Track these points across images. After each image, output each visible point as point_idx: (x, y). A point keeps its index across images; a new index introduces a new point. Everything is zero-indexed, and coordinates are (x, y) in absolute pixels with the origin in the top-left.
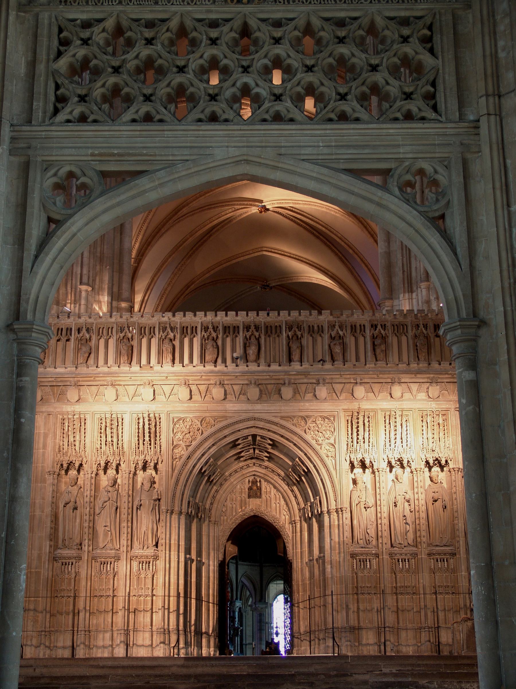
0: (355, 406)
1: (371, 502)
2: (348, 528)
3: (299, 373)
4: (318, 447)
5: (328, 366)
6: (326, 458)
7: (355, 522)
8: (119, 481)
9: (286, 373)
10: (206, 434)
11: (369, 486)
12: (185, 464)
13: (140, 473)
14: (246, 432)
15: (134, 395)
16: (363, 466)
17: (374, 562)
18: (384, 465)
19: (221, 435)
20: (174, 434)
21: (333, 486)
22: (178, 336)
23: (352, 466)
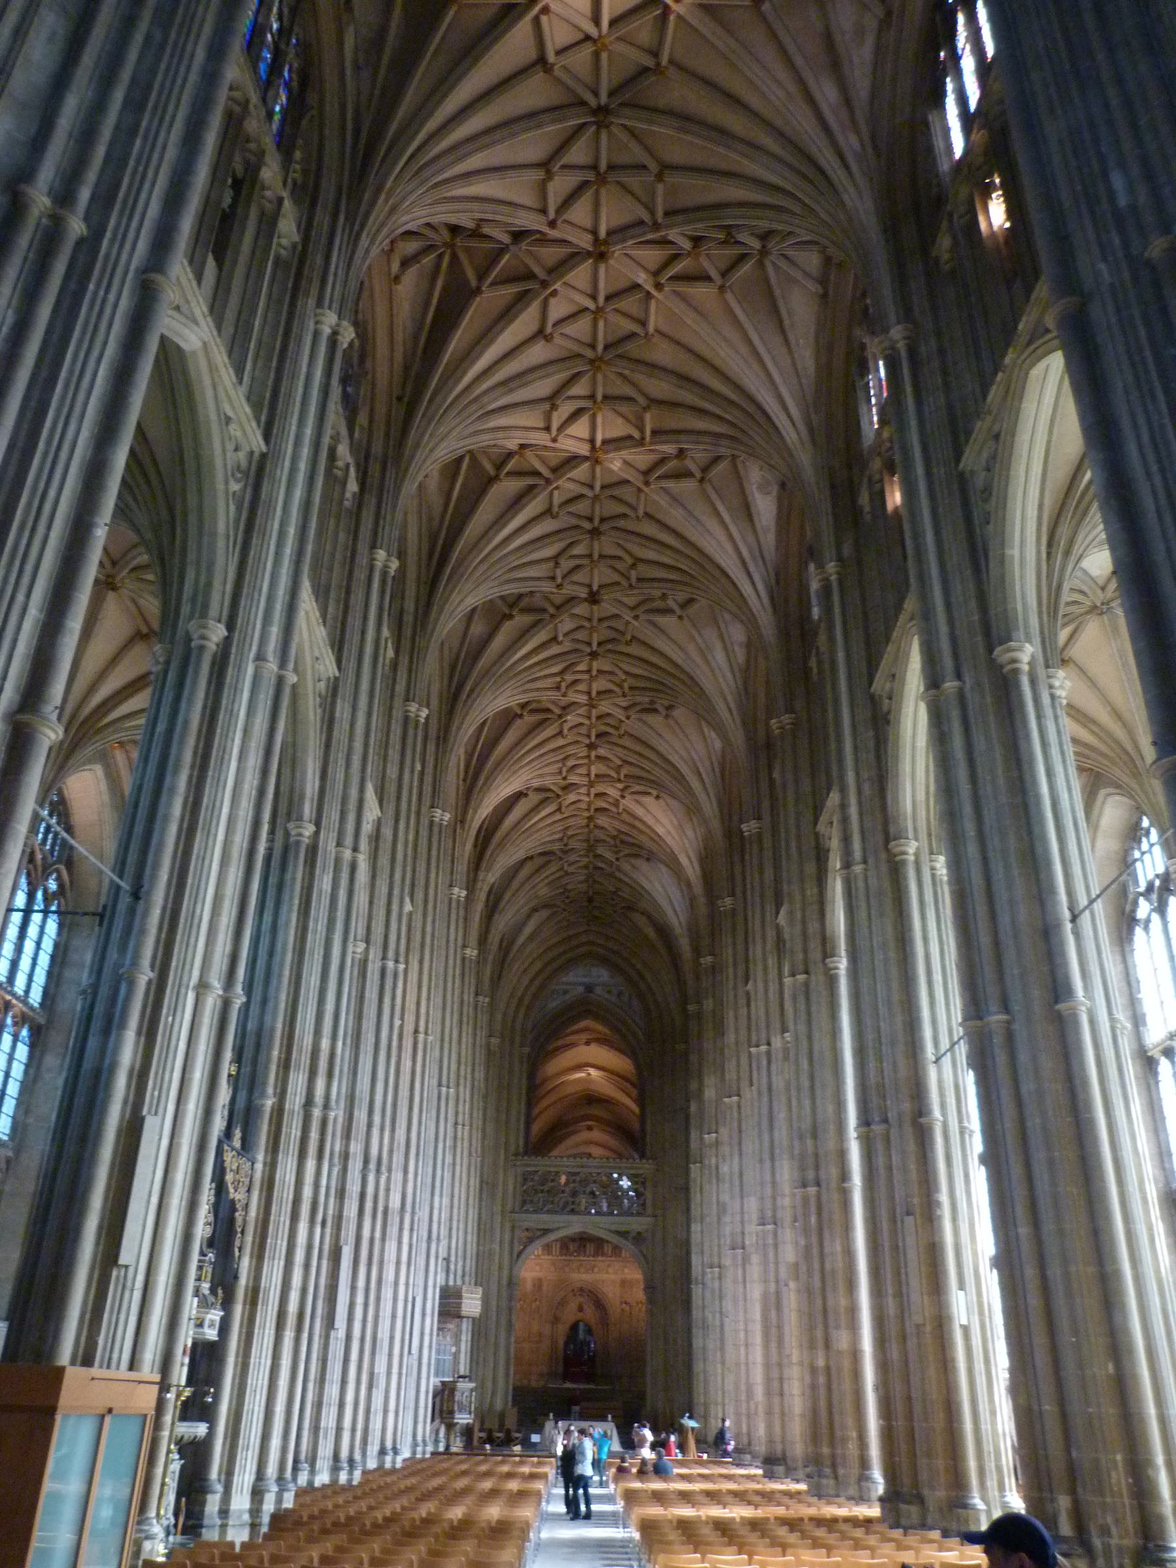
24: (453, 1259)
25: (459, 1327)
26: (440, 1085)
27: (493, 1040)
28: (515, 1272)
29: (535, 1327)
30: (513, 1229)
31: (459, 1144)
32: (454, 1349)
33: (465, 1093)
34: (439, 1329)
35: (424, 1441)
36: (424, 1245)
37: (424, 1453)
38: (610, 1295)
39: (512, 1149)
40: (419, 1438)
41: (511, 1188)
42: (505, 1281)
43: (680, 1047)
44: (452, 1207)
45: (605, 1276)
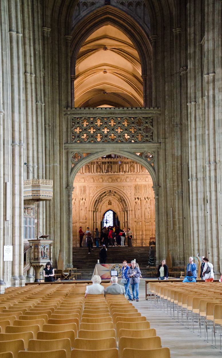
0: (136, 183)
1: (140, 208)
2: (134, 215)
3: (122, 175)
4: (127, 194)
5: (129, 173)
6: (129, 197)
7: (136, 213)
8: (76, 203)
9: (118, 175)
10: (98, 190)
11: (140, 204)
12: (93, 198)
13: (81, 200)
14: (108, 190)
15: (79, 180)
16: (138, 199)
17: (140, 223)
18: (143, 199)
19: (101, 191)
20: (90, 191)
21: (130, 204)
22: (90, 165)
23: (135, 199)
24: (31, 163)
25: (38, 206)
26: (10, 30)
27: (46, 29)
28: (70, 179)
29: (83, 213)
30: (67, 153)
31: (29, 86)
32: (36, 221)
33: (30, 50)
34: (25, 208)
35: (20, 276)
36: (10, 147)
37: (21, 284)
38: (129, 195)
39: (64, 103)
40: (17, 274)
41: (64, 130)
42: (64, 186)
43: (176, 31)
44: (27, 130)
45: (124, 184)
